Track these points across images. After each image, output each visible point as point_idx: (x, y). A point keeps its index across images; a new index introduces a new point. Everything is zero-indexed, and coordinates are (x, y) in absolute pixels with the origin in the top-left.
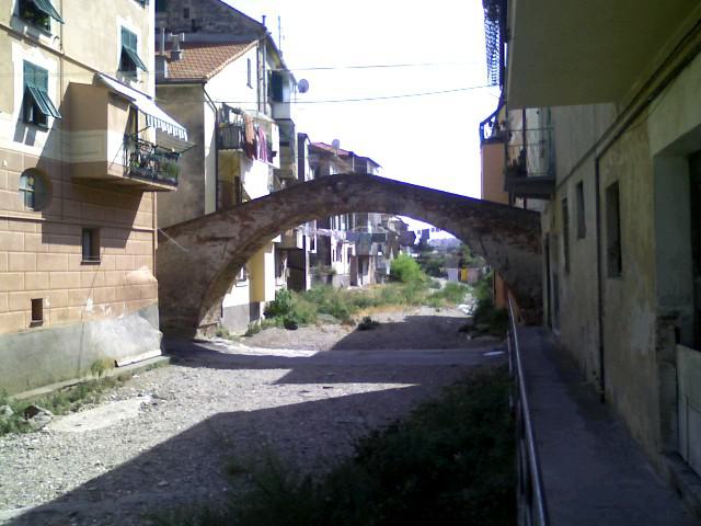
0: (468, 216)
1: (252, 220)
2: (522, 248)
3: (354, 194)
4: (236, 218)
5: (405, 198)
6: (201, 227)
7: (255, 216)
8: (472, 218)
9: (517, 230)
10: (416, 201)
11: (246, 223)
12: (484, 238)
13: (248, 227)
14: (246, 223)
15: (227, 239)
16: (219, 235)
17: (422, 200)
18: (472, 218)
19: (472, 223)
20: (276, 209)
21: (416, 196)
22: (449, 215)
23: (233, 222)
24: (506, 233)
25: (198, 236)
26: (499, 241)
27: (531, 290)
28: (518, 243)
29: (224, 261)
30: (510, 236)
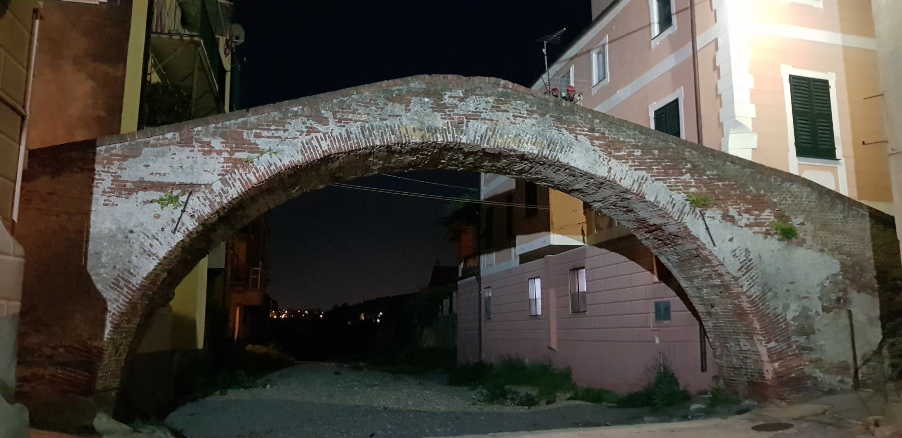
0: (682, 174)
1: (254, 149)
2: (767, 233)
3: (475, 116)
4: (217, 143)
5: (571, 131)
6: (125, 158)
7: (262, 143)
8: (687, 177)
9: (758, 203)
10: (592, 139)
11: (237, 155)
12: (708, 213)
13: (246, 163)
14: (237, 155)
15: (190, 189)
16: (171, 179)
17: (603, 136)
18: (687, 177)
19: (687, 185)
20: (311, 130)
21: (592, 130)
22: (649, 169)
23: (208, 150)
24: (743, 206)
25: (116, 179)
26: (732, 220)
27: (786, 307)
28: (758, 225)
29: (179, 237)
30: (747, 211)
